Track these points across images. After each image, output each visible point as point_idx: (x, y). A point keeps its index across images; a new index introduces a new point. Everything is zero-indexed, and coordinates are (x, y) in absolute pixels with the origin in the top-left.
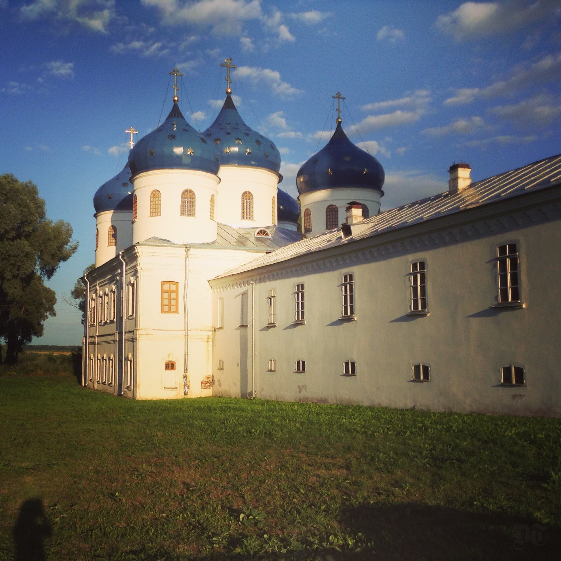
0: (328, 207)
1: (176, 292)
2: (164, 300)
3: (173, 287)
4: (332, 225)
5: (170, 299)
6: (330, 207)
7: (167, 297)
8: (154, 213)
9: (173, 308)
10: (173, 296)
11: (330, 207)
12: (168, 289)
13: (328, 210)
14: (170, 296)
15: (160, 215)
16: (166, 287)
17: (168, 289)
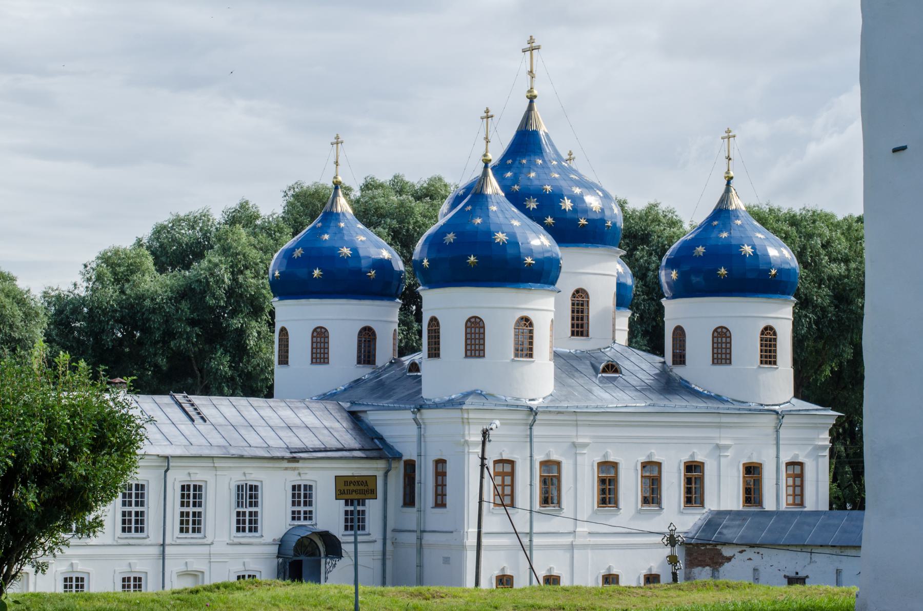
0: (716, 330)
1: (512, 474)
2: (505, 487)
3: (508, 468)
4: (722, 359)
5: (503, 485)
6: (719, 330)
7: (500, 483)
8: (473, 352)
9: (507, 501)
10: (508, 480)
12: (502, 470)
13: (716, 334)
14: (503, 481)
15: (484, 356)
16: (499, 468)
17: (502, 470)
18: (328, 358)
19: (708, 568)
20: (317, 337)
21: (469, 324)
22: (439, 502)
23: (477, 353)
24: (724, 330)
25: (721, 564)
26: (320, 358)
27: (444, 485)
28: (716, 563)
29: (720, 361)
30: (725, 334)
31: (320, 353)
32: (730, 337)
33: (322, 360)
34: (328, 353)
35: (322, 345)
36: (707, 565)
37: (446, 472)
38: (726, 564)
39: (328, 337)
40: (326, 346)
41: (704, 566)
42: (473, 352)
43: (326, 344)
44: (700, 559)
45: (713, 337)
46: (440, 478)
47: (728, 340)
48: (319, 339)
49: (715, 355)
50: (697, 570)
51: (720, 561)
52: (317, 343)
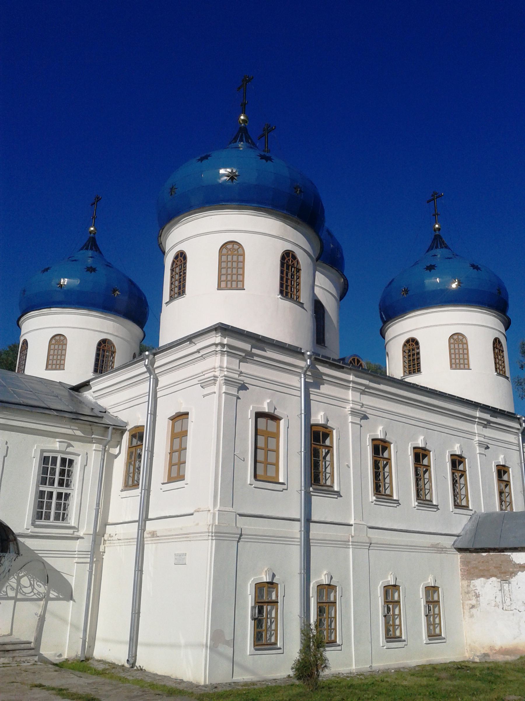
0: (452, 337)
8: (229, 283)
11: (455, 337)
13: (452, 341)
18: (64, 365)
19: (494, 579)
20: (55, 345)
21: (224, 251)
22: (174, 474)
23: (234, 284)
24: (461, 337)
25: (513, 574)
26: (56, 364)
27: (182, 449)
28: (505, 573)
29: (458, 365)
30: (462, 340)
31: (57, 359)
32: (467, 344)
33: (58, 366)
34: (64, 360)
35: (60, 351)
36: (495, 576)
37: (187, 431)
38: (520, 573)
39: (66, 345)
40: (63, 353)
41: (488, 577)
42: (229, 283)
43: (64, 346)
44: (481, 568)
45: (450, 344)
46: (177, 441)
47: (465, 346)
48: (56, 347)
49: (453, 361)
50: (478, 583)
51: (511, 570)
52: (54, 350)
